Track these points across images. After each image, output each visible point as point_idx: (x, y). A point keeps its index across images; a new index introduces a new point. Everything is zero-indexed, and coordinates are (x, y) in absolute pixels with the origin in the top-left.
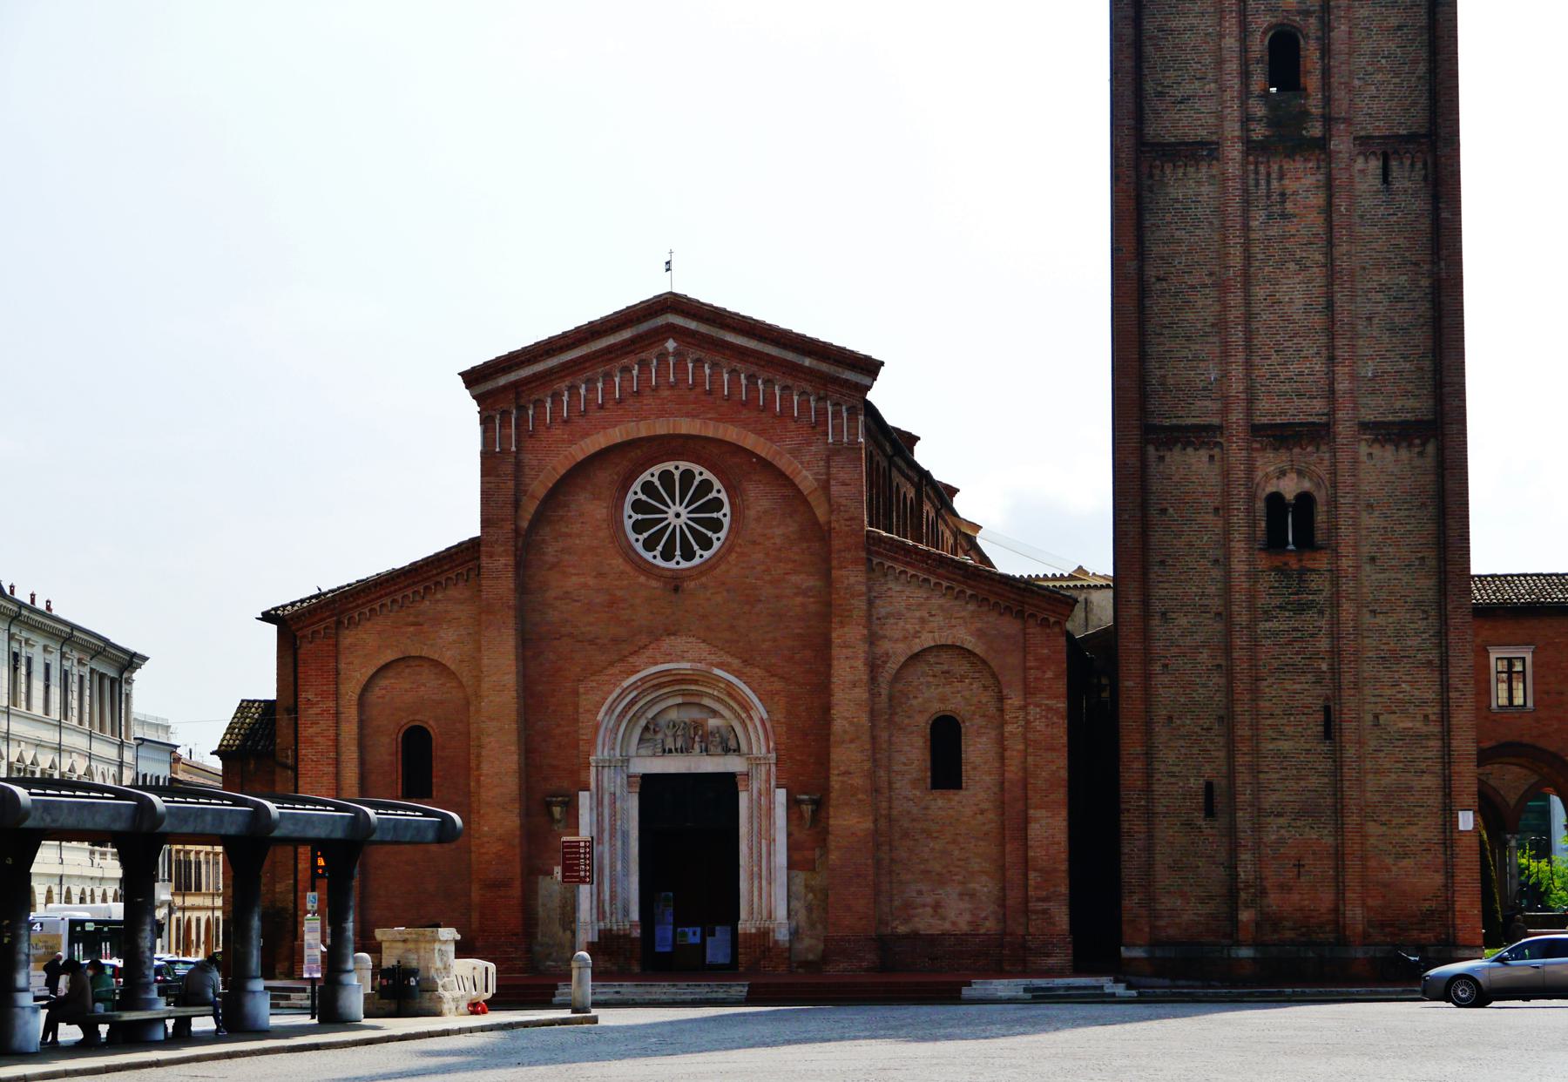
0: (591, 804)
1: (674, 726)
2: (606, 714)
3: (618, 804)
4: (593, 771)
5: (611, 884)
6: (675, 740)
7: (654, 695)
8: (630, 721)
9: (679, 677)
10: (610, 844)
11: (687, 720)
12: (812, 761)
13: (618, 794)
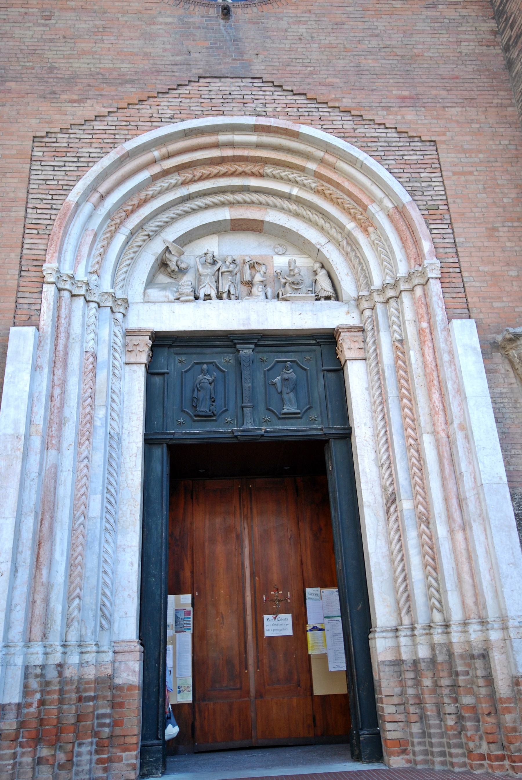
0: (35, 358)
1: (214, 262)
2: (86, 196)
3: (102, 375)
4: (49, 291)
5: (72, 546)
6: (217, 282)
7: (184, 191)
8: (132, 234)
9: (229, 152)
10: (78, 453)
11: (235, 258)
12: (514, 273)
13: (103, 355)
